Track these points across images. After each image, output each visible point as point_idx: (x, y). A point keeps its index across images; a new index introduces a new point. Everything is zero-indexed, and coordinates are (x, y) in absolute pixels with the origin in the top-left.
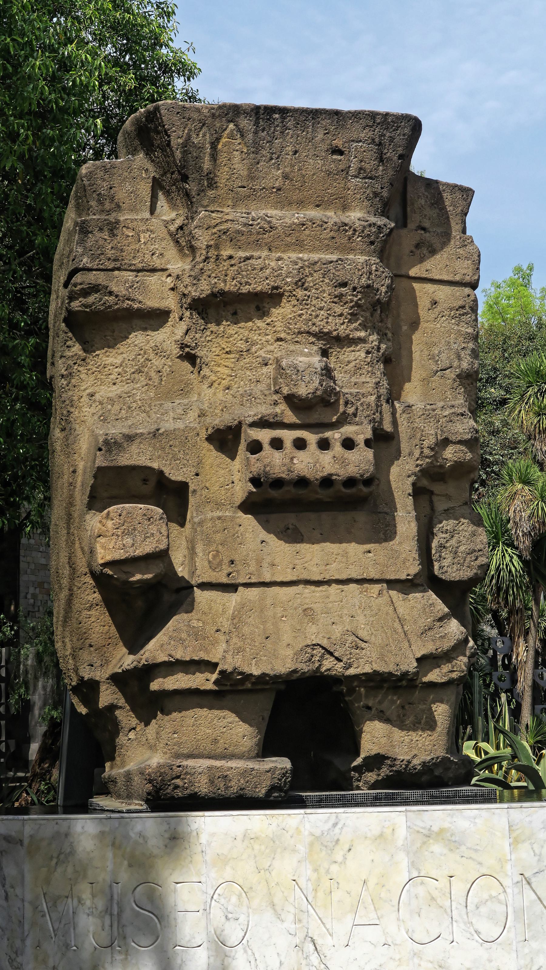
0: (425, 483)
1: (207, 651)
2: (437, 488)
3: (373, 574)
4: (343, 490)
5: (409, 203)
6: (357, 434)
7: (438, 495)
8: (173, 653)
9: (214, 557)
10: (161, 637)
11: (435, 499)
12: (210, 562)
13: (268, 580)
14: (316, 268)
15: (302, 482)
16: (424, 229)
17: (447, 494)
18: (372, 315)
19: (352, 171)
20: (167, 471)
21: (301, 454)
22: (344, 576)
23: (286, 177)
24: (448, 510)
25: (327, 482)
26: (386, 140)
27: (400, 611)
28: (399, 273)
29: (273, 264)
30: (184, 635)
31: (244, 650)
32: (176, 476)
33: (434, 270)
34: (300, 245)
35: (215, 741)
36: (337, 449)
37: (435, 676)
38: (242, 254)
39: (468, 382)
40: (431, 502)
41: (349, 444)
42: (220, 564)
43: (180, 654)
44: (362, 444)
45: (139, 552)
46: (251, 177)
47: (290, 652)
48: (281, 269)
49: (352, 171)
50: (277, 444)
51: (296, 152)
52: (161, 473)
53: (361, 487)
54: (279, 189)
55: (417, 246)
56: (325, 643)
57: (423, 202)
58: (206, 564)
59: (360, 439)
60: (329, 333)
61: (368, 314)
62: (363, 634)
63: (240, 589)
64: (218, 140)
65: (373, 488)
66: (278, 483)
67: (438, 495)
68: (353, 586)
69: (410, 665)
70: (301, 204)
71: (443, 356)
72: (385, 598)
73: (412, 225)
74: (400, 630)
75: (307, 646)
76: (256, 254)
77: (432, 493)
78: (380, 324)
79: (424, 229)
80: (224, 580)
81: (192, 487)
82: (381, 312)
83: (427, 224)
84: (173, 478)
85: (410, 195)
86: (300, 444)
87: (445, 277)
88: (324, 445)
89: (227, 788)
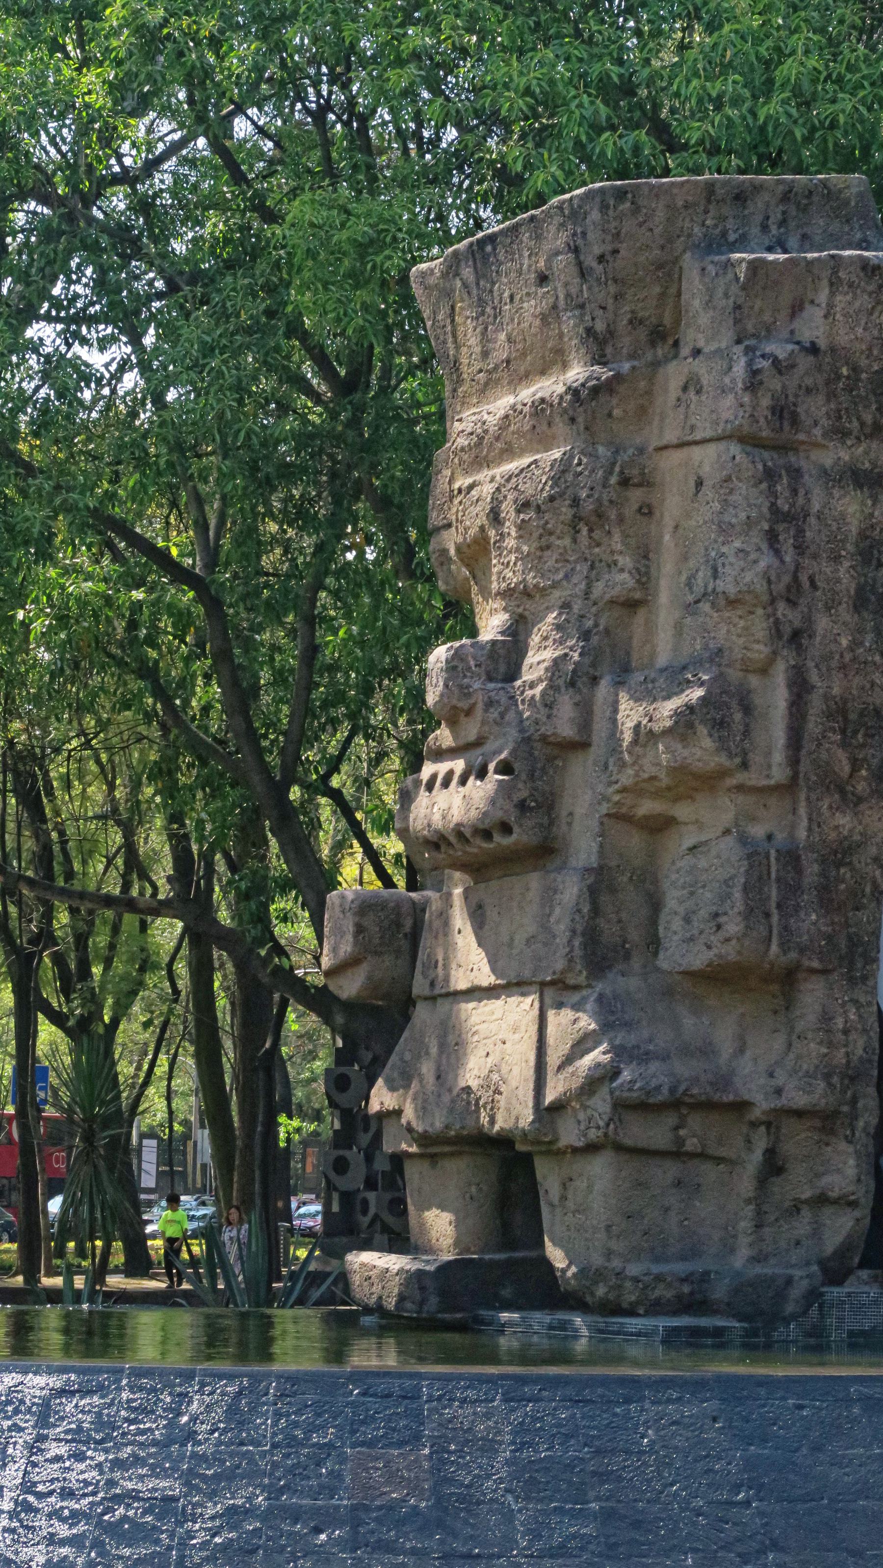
2: (682, 811)
7: (686, 824)
17: (697, 821)
18: (575, 541)
19: (562, 303)
24: (695, 847)
26: (580, 242)
33: (699, 424)
34: (509, 453)
37: (569, 1134)
38: (469, 481)
39: (739, 612)
46: (485, 354)
49: (562, 303)
51: (512, 297)
53: (497, 838)
54: (508, 362)
55: (685, 389)
60: (514, 589)
61: (567, 541)
64: (453, 308)
67: (686, 824)
70: (526, 377)
76: (480, 477)
78: (597, 550)
80: (427, 992)
82: (591, 530)
83: (701, 343)
87: (708, 434)
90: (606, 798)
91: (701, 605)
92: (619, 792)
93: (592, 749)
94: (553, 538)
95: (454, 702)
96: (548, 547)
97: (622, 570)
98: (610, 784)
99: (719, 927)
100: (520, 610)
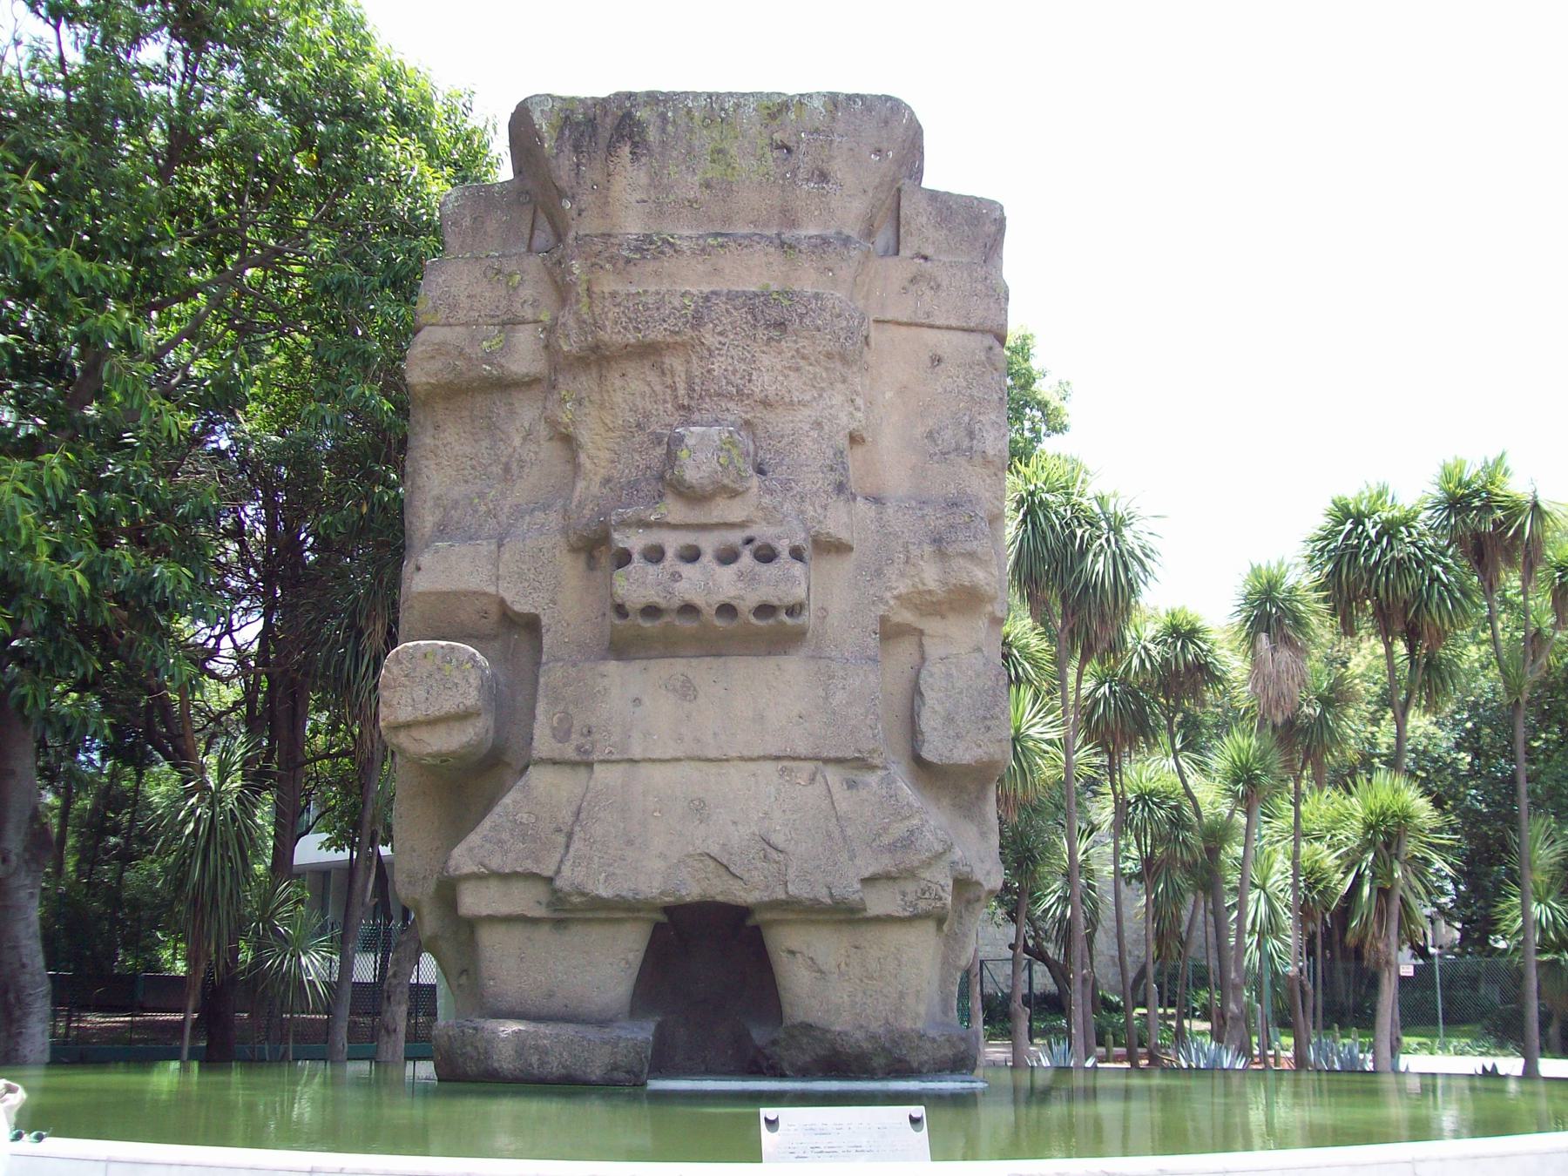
0: (906, 616)
1: (537, 861)
2: (931, 626)
3: (802, 750)
4: (753, 620)
5: (903, 221)
6: (780, 538)
9: (561, 720)
10: (474, 838)
11: (926, 641)
12: (554, 729)
14: (739, 302)
15: (689, 609)
16: (926, 258)
21: (687, 570)
22: (757, 753)
23: (707, 185)
25: (727, 610)
27: (843, 807)
29: (676, 304)
30: (505, 836)
31: (591, 859)
32: (521, 606)
35: (551, 995)
36: (746, 559)
40: (921, 645)
41: (766, 555)
42: (568, 733)
43: (495, 863)
44: (785, 554)
45: (434, 711)
47: (659, 864)
48: (685, 307)
50: (655, 555)
52: (502, 602)
53: (784, 617)
55: (913, 280)
56: (714, 850)
57: (924, 220)
58: (548, 731)
59: (783, 547)
62: (778, 839)
63: (596, 767)
65: (800, 621)
66: (651, 611)
68: (770, 767)
69: (850, 889)
71: (948, 434)
72: (818, 788)
73: (905, 252)
74: (837, 834)
75: (689, 856)
77: (921, 633)
79: (926, 258)
80: (571, 754)
81: (545, 621)
83: (929, 251)
84: (517, 608)
85: (905, 211)
86: (691, 555)
87: (954, 323)
88: (728, 557)
89: (542, 1063)
90: (881, 599)
91: (952, 456)
92: (897, 598)
93: (854, 555)
94: (802, 363)
95: (726, 481)
96: (797, 369)
97: (858, 409)
98: (890, 589)
99: (988, 728)
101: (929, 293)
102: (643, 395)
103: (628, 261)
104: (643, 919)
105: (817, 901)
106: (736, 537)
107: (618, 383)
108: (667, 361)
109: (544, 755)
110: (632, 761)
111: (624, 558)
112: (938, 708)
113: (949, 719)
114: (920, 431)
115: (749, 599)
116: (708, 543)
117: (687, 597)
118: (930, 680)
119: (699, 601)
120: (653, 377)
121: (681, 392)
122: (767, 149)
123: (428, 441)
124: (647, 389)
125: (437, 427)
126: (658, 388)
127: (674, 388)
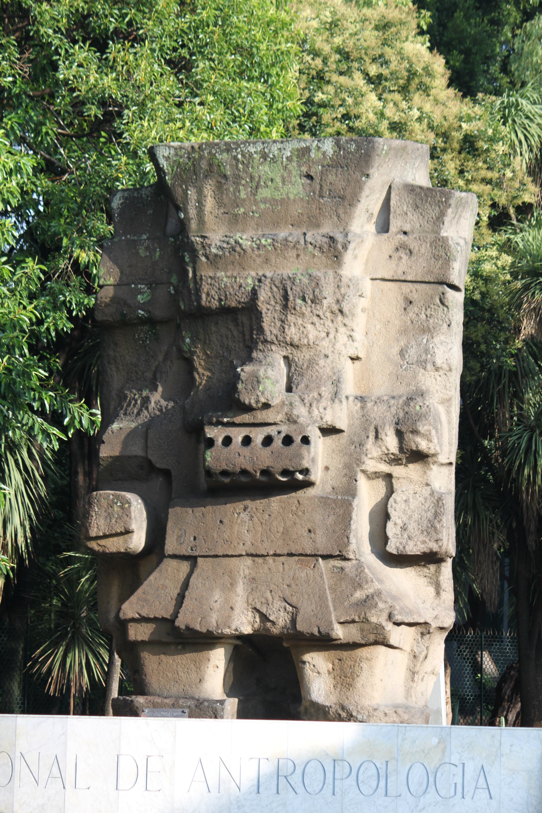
8: (140, 612)
10: (133, 598)
13: (220, 554)
16: (405, 233)
20: (153, 459)
28: (374, 277)
79: (405, 233)
100: (285, 354)
101: (405, 257)
102: (227, 337)
103: (216, 255)
104: (229, 643)
105: (312, 634)
106: (271, 431)
107: (214, 329)
108: (239, 317)
109: (171, 553)
110: (216, 556)
111: (211, 443)
112: (399, 522)
113: (404, 528)
114: (396, 350)
115: (277, 467)
116: (258, 435)
117: (243, 467)
118: (394, 505)
119: (249, 468)
120: (231, 326)
121: (247, 337)
122: (298, 178)
123: (111, 353)
124: (229, 333)
125: (116, 344)
126: (235, 333)
127: (243, 333)
